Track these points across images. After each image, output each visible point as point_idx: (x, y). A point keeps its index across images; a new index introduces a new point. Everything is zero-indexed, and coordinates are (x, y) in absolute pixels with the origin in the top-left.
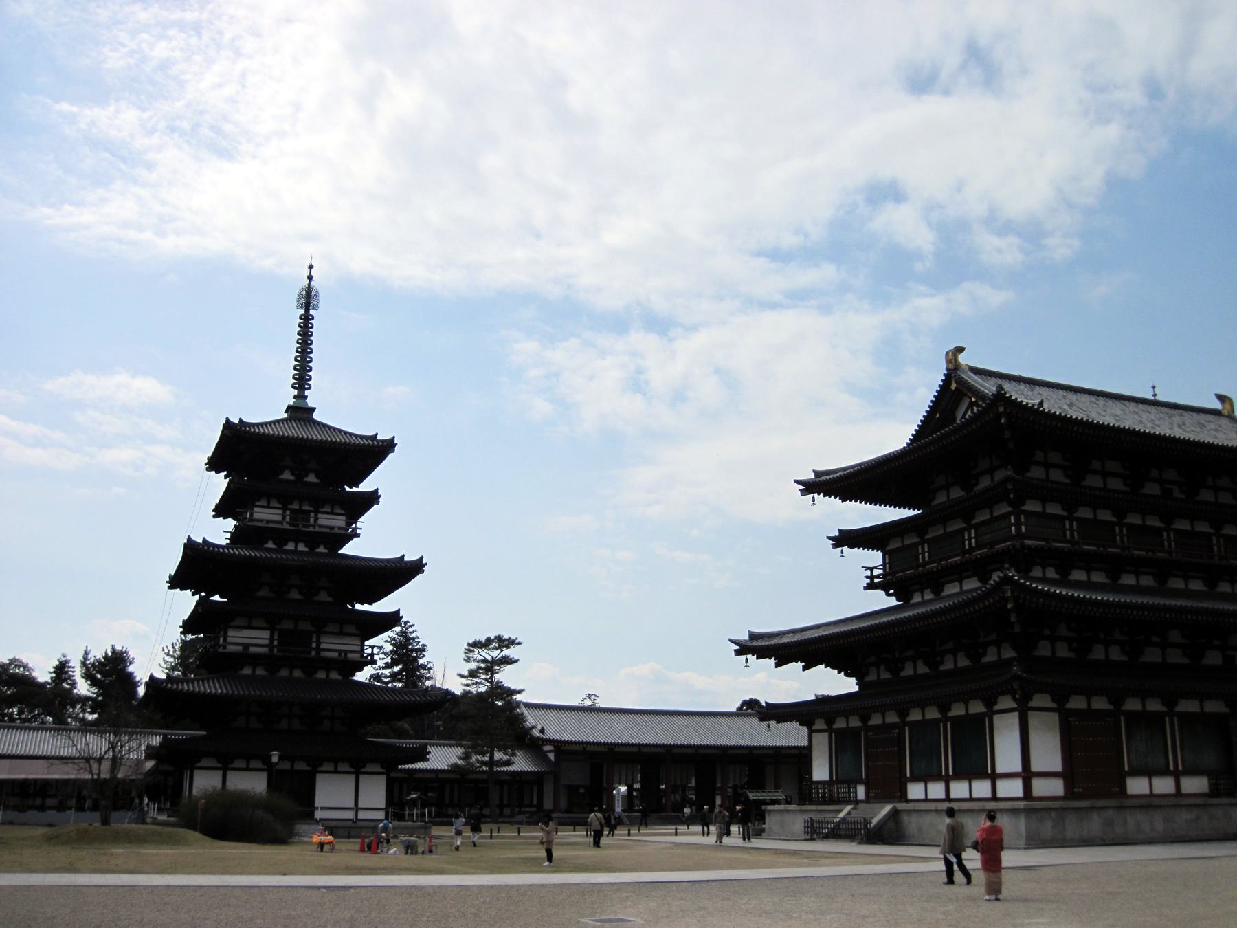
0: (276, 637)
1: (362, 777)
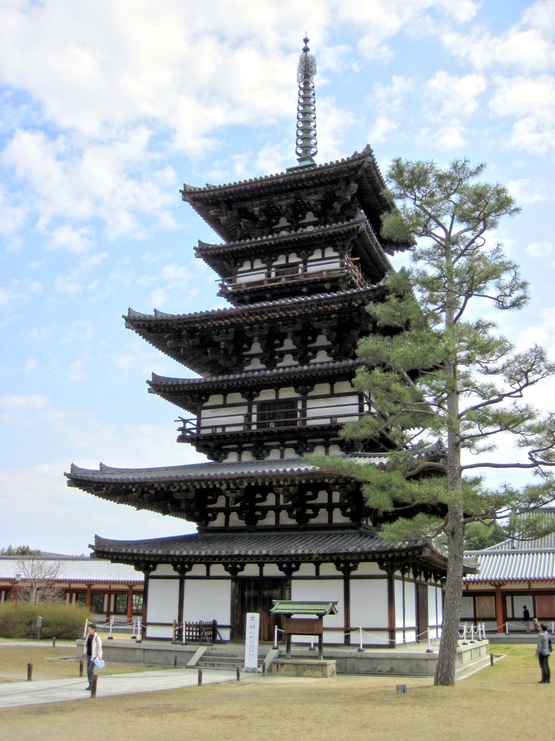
0: (254, 410)
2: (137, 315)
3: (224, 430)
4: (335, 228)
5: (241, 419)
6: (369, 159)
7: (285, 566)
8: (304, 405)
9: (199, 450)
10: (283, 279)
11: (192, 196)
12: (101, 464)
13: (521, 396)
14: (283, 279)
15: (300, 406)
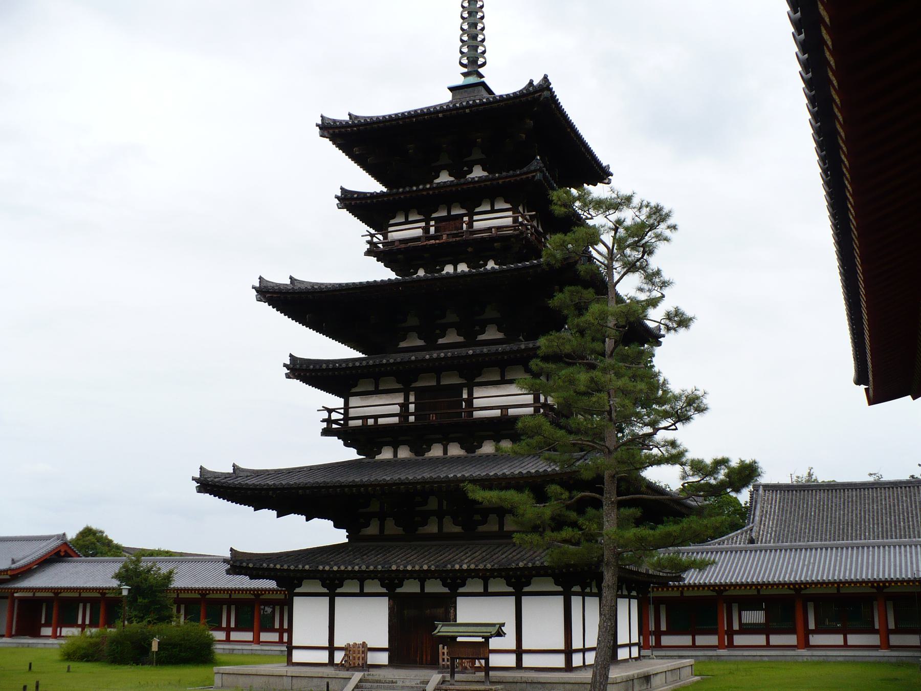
0: (412, 398)
1: (525, 599)
2: (269, 284)
3: (376, 421)
4: (506, 177)
5: (396, 409)
6: (546, 93)
7: (449, 581)
8: (470, 394)
9: (346, 445)
10: (445, 237)
11: (331, 131)
12: (234, 466)
13: (676, 429)
14: (445, 237)
15: (465, 396)
